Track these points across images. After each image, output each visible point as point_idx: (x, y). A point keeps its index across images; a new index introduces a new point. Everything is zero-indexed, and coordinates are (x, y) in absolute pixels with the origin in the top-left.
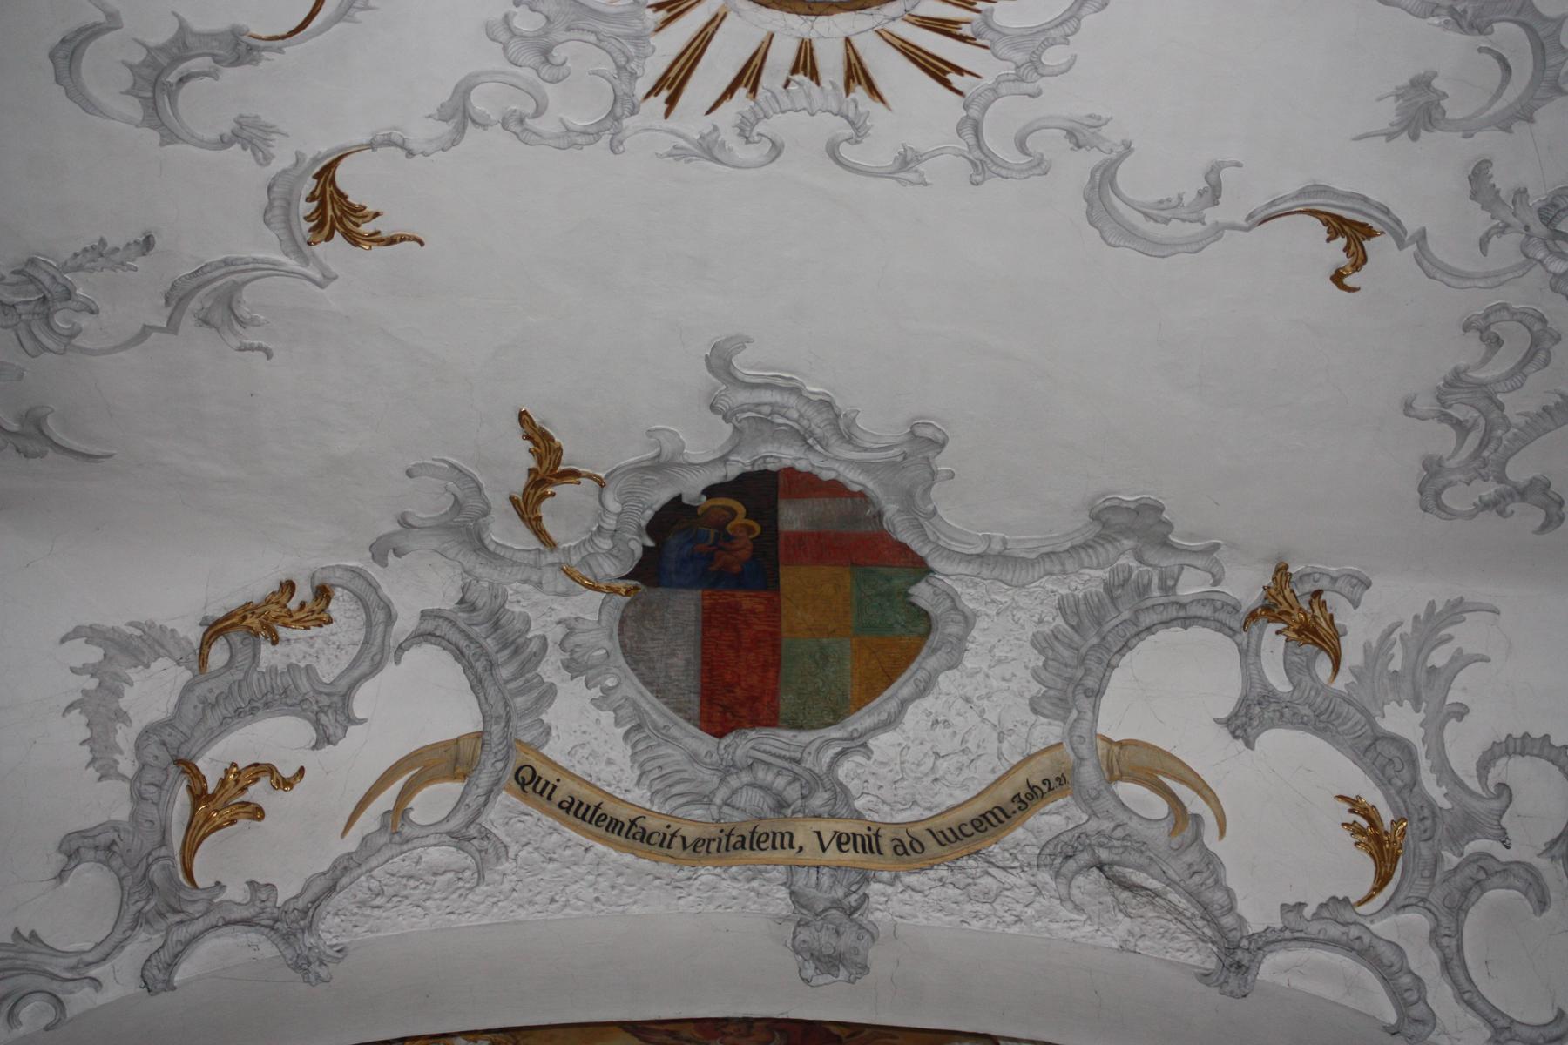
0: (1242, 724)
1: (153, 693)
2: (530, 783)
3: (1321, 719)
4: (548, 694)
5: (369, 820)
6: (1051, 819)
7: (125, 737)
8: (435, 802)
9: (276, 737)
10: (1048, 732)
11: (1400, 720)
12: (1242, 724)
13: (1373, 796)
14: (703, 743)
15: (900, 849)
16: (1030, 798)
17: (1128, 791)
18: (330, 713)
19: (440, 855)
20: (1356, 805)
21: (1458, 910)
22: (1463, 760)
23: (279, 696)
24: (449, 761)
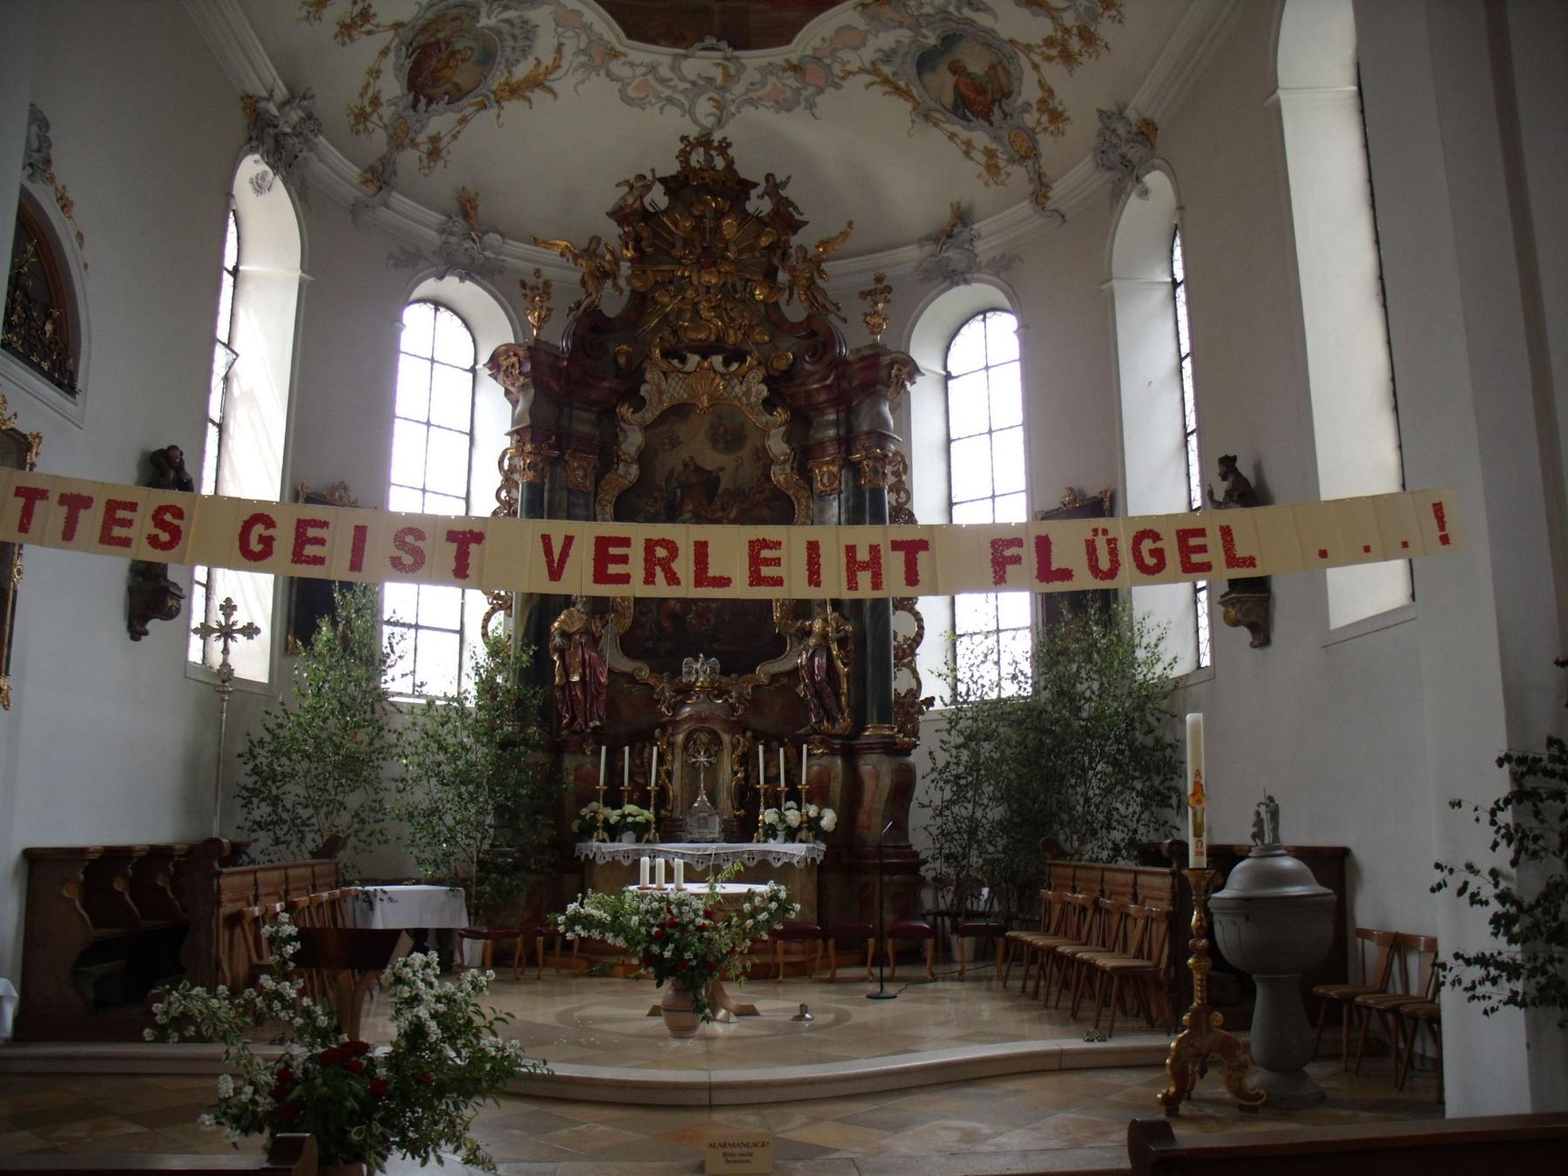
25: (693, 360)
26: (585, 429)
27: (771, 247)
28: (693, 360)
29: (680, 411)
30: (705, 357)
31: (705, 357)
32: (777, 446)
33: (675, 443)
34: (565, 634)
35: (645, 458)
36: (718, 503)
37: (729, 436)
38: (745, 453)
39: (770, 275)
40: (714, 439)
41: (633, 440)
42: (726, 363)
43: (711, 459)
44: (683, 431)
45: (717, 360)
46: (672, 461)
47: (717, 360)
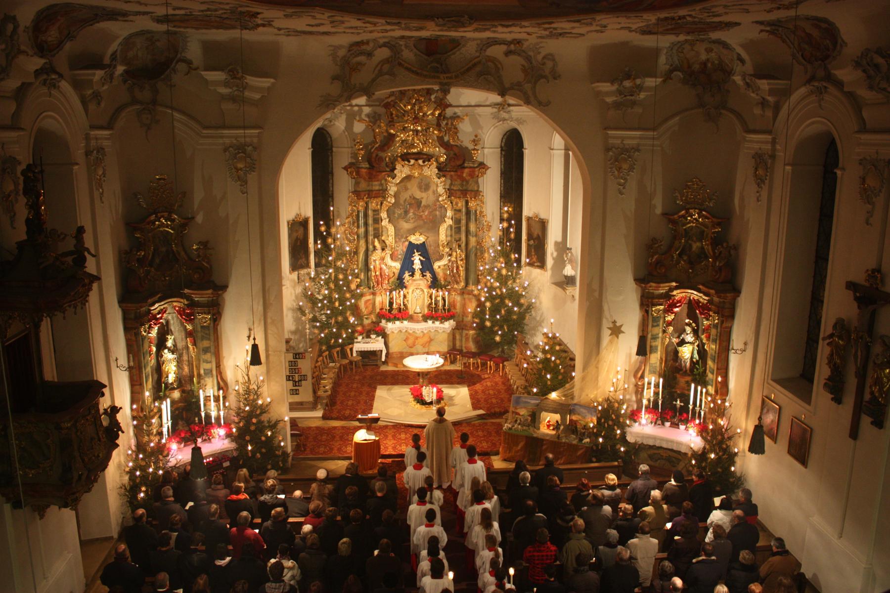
0: (508, 53)
1: (342, 53)
2: (400, 64)
3: (519, 55)
4: (402, 51)
5: (376, 72)
6: (478, 68)
7: (338, 59)
8: (386, 67)
9: (362, 59)
10: (478, 54)
11: (531, 53)
12: (508, 53)
13: (526, 65)
14: (426, 57)
15: (456, 77)
16: (475, 65)
17: (490, 64)
18: (370, 55)
19: (387, 77)
20: (523, 66)
21: (535, 83)
22: (540, 57)
23: (362, 53)
24: (387, 61)
25: (412, 162)
26: (377, 188)
27: (440, 114)
28: (412, 162)
29: (408, 178)
30: (416, 160)
31: (416, 160)
32: (441, 190)
33: (406, 189)
34: (375, 261)
35: (396, 196)
36: (421, 209)
37: (425, 186)
38: (430, 192)
39: (438, 125)
40: (420, 188)
41: (392, 189)
42: (424, 162)
43: (418, 195)
44: (409, 185)
45: (420, 162)
46: (405, 196)
47: (420, 162)
